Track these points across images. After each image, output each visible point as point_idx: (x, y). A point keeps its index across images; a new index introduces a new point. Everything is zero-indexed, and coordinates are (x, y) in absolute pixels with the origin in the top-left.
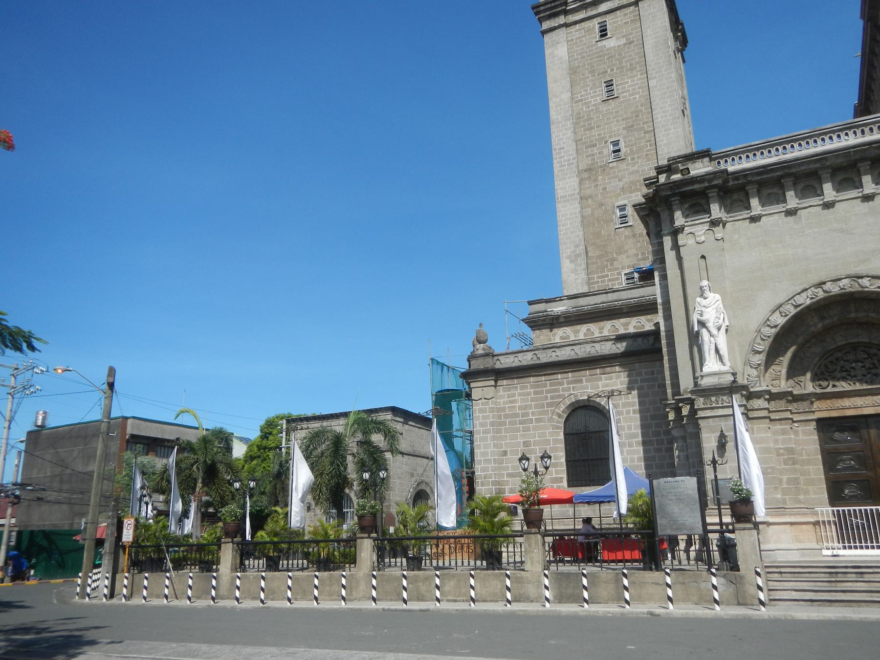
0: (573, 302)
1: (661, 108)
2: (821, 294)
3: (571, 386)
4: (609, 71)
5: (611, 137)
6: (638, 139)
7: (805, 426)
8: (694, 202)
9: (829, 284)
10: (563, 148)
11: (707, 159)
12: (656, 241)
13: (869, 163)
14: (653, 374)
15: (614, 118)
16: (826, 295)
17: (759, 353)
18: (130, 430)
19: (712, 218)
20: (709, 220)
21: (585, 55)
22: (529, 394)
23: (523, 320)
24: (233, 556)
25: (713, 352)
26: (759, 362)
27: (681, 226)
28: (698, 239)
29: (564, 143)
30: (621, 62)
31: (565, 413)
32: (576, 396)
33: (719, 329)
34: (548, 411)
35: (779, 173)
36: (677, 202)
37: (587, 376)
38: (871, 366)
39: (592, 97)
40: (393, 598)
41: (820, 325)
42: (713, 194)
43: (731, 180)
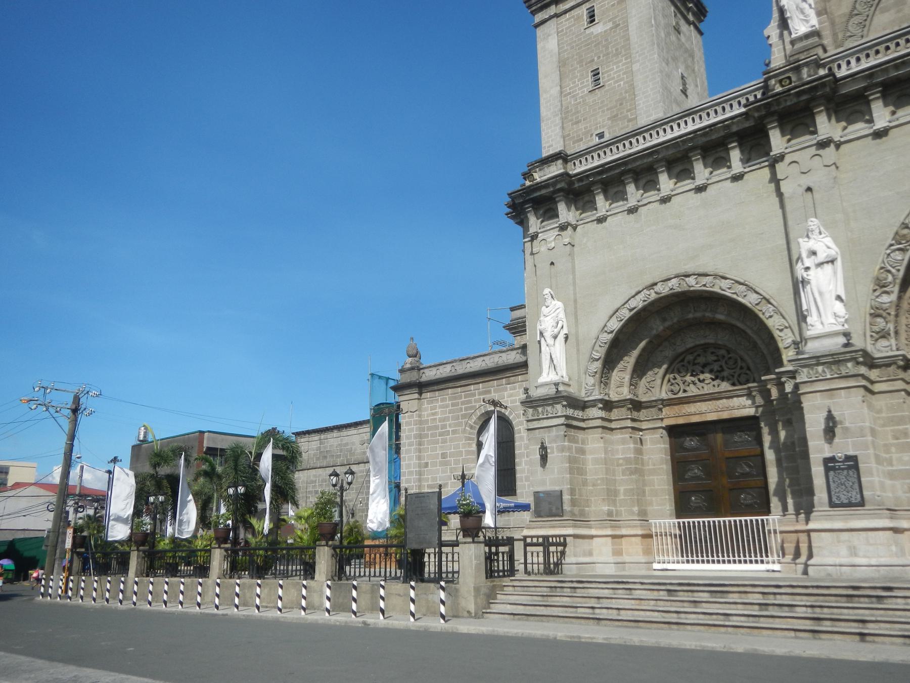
2: (653, 296)
4: (596, 58)
5: (596, 129)
6: (622, 129)
7: (653, 434)
8: (548, 207)
9: (659, 284)
16: (658, 296)
17: (597, 360)
18: (205, 445)
21: (574, 44)
22: (447, 406)
23: (504, 327)
24: (138, 562)
26: (595, 371)
27: (534, 233)
28: (549, 245)
29: (552, 141)
30: (607, 48)
31: (477, 424)
33: (555, 337)
37: (494, 386)
38: (719, 369)
39: (579, 89)
40: (229, 603)
41: (661, 328)
43: (576, 182)
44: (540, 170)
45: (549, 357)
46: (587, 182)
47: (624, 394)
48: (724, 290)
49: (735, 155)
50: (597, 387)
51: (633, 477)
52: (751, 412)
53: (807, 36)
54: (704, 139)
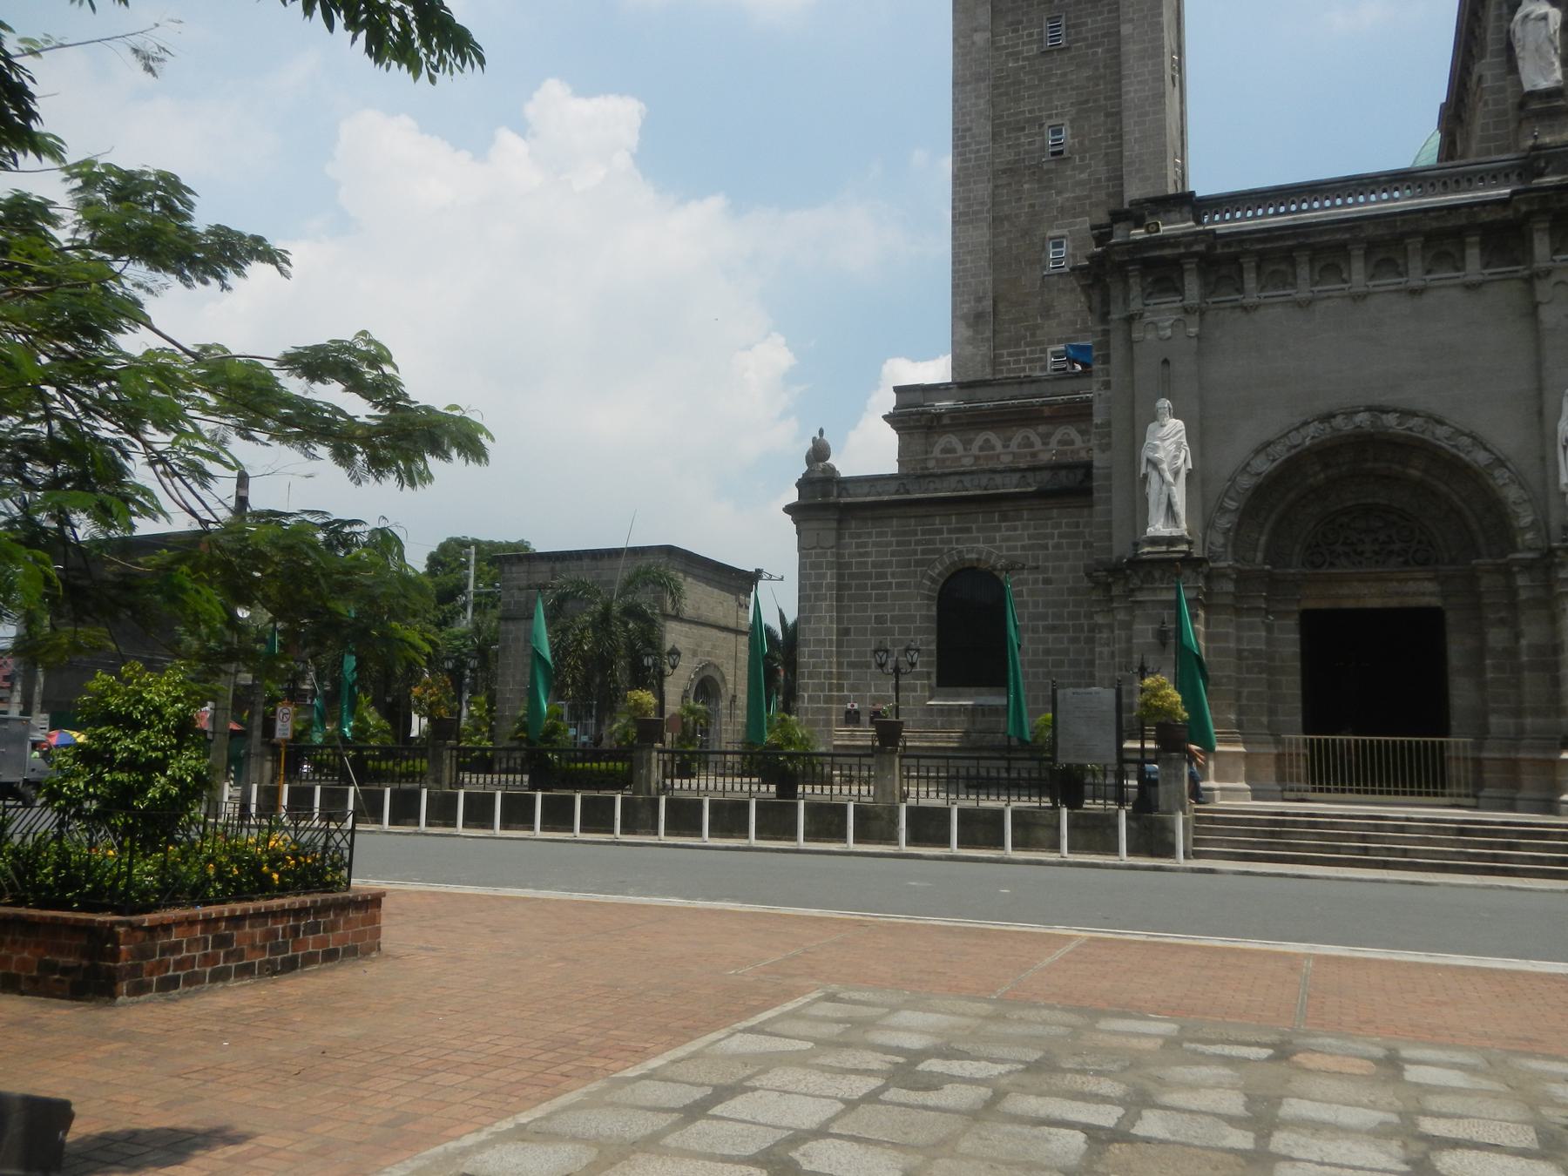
0: (965, 393)
1: (1136, 76)
3: (954, 536)
5: (1050, 117)
10: (970, 129)
11: (1186, 209)
12: (1099, 328)
13: (1422, 239)
14: (1078, 526)
15: (1058, 84)
19: (1185, 302)
20: (1180, 304)
22: (889, 544)
23: (886, 418)
25: (1163, 507)
26: (1228, 526)
28: (1162, 333)
29: (971, 121)
32: (960, 552)
34: (916, 571)
35: (1290, 243)
36: (1136, 273)
39: (1024, 44)
42: (1190, 265)
43: (1219, 247)
44: (1152, 214)
45: (1165, 500)
46: (1239, 249)
47: (1257, 561)
48: (1438, 439)
49: (1473, 257)
50: (1230, 549)
51: (1264, 676)
52: (1435, 602)
53: (1549, 94)
54: (1435, 224)
